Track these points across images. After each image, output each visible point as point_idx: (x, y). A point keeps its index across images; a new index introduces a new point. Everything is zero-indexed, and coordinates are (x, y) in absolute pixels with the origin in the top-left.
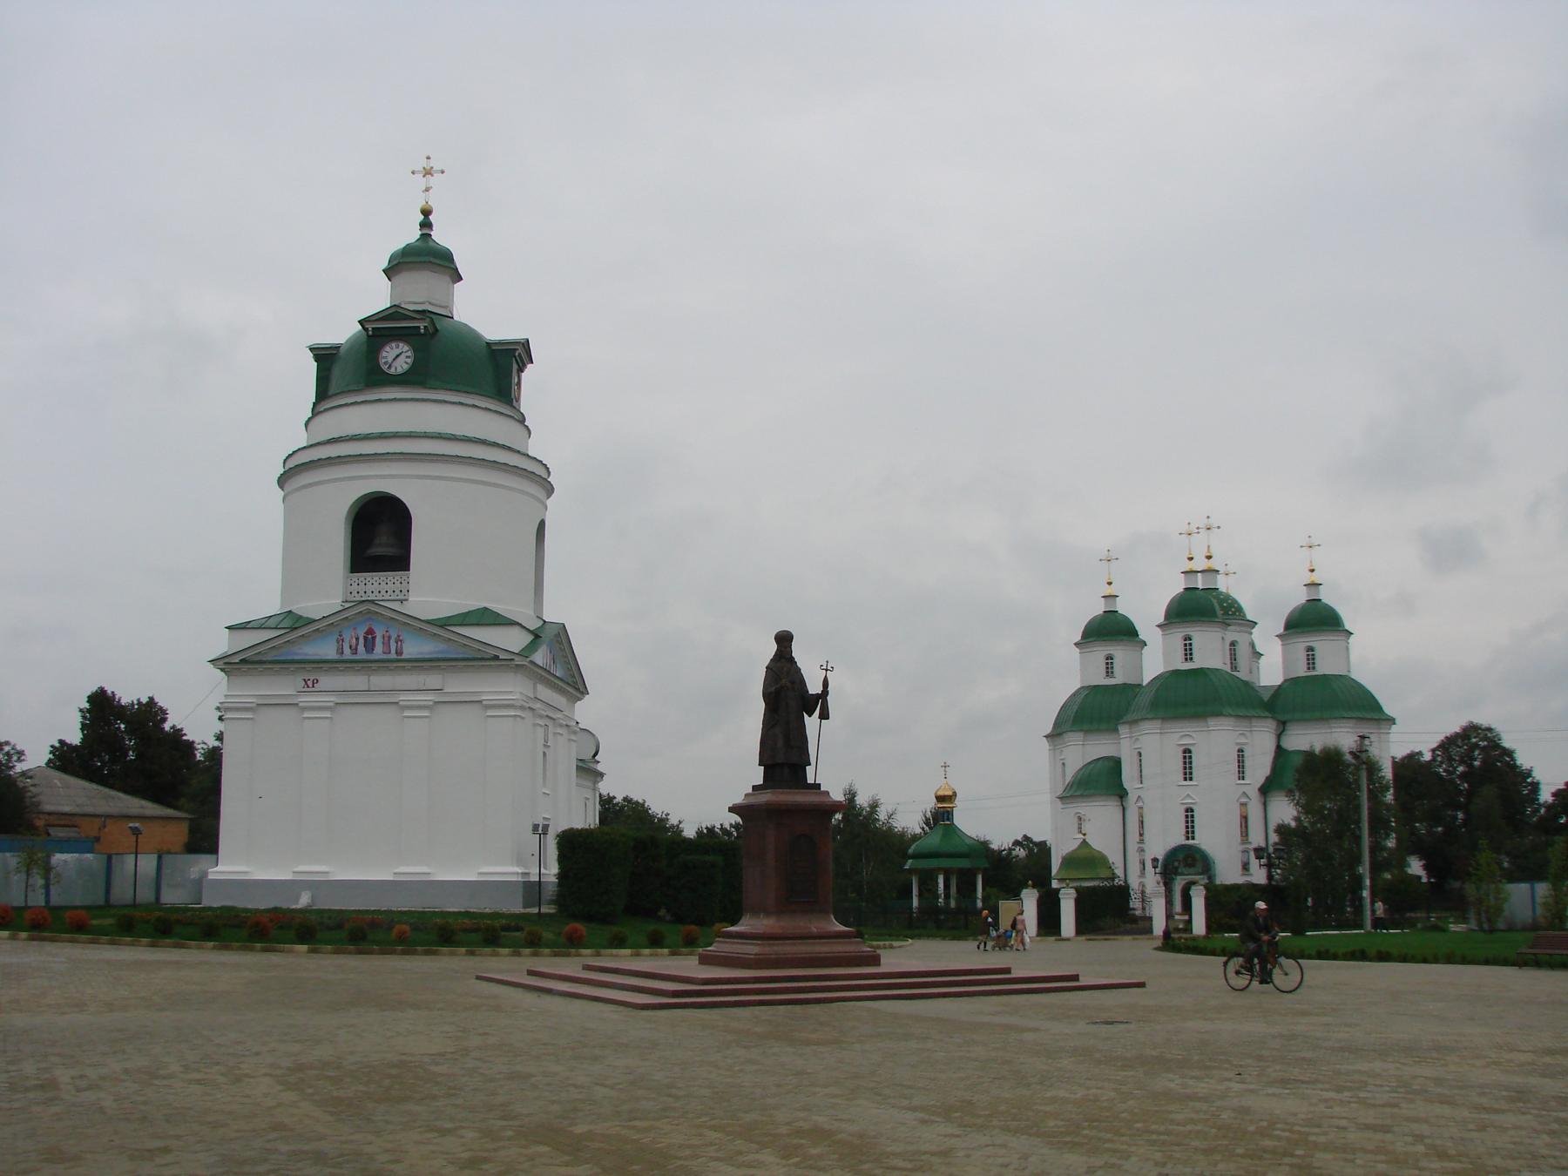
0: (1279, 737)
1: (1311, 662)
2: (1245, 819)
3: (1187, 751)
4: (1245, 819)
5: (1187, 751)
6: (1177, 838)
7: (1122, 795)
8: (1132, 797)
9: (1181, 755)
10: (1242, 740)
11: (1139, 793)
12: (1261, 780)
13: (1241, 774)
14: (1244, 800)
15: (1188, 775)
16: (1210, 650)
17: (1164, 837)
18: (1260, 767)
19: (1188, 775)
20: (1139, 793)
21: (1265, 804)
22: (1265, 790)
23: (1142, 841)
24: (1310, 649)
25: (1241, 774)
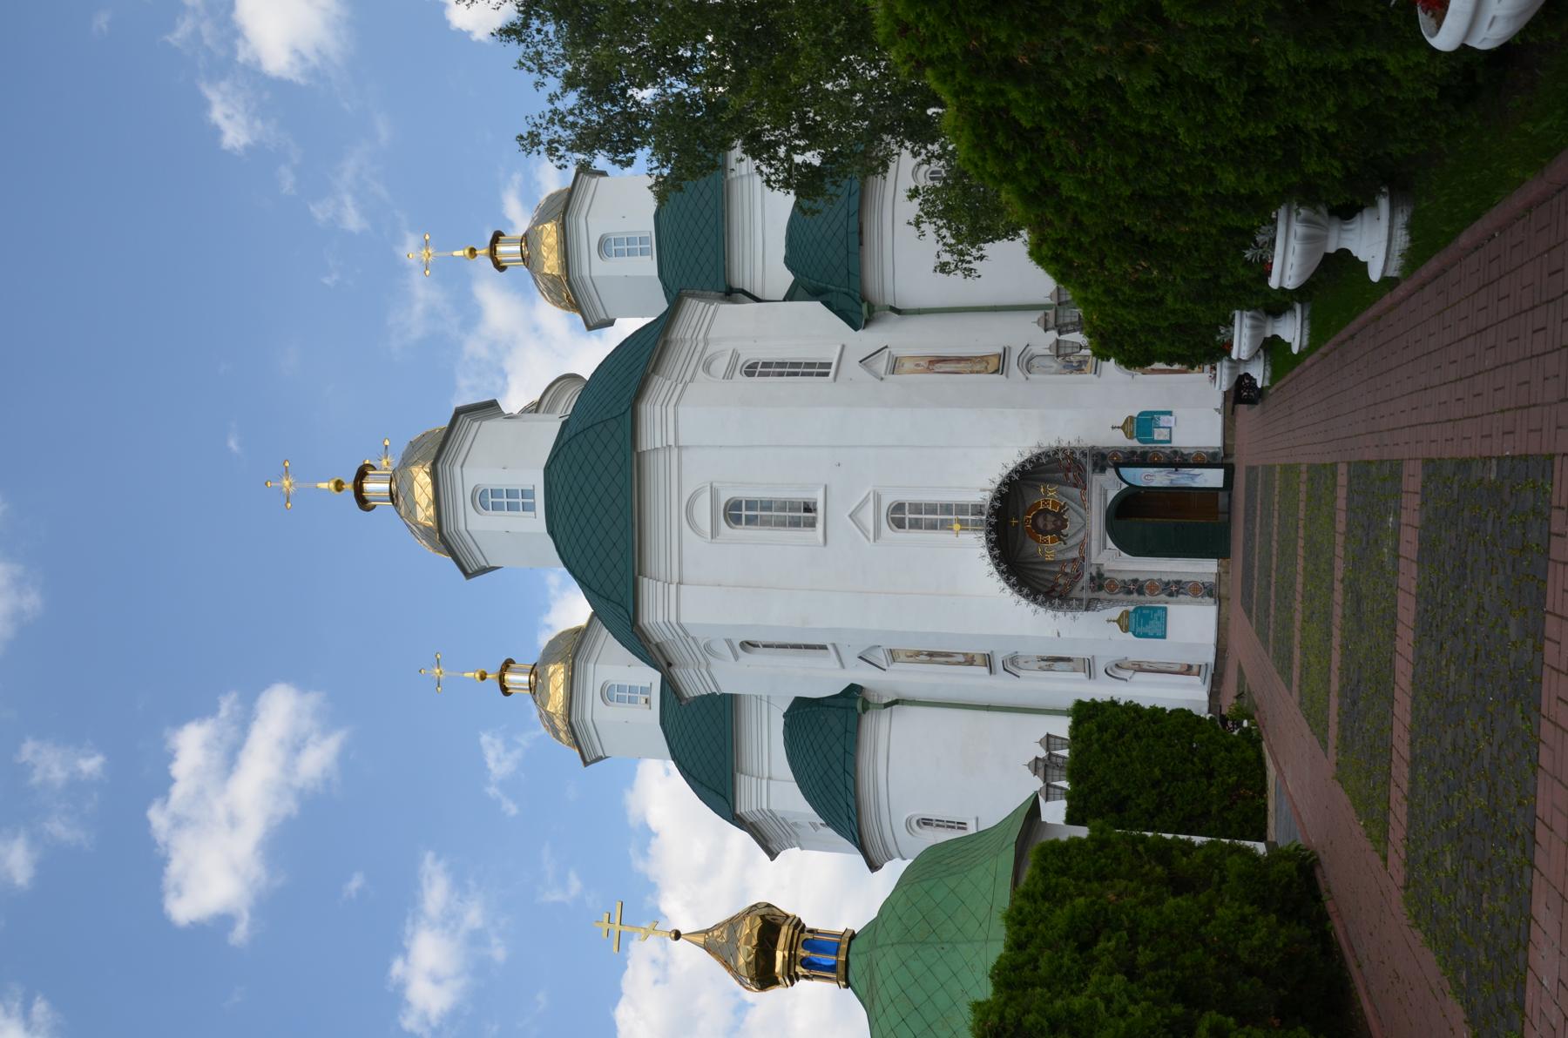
0: (758, 300)
2: (936, 363)
4: (936, 363)
5: (736, 513)
6: (970, 554)
8: (863, 675)
9: (742, 532)
10: (720, 366)
11: (850, 658)
13: (819, 369)
14: (882, 364)
18: (814, 328)
20: (850, 658)
23: (988, 661)
24: (603, 244)
25: (819, 369)
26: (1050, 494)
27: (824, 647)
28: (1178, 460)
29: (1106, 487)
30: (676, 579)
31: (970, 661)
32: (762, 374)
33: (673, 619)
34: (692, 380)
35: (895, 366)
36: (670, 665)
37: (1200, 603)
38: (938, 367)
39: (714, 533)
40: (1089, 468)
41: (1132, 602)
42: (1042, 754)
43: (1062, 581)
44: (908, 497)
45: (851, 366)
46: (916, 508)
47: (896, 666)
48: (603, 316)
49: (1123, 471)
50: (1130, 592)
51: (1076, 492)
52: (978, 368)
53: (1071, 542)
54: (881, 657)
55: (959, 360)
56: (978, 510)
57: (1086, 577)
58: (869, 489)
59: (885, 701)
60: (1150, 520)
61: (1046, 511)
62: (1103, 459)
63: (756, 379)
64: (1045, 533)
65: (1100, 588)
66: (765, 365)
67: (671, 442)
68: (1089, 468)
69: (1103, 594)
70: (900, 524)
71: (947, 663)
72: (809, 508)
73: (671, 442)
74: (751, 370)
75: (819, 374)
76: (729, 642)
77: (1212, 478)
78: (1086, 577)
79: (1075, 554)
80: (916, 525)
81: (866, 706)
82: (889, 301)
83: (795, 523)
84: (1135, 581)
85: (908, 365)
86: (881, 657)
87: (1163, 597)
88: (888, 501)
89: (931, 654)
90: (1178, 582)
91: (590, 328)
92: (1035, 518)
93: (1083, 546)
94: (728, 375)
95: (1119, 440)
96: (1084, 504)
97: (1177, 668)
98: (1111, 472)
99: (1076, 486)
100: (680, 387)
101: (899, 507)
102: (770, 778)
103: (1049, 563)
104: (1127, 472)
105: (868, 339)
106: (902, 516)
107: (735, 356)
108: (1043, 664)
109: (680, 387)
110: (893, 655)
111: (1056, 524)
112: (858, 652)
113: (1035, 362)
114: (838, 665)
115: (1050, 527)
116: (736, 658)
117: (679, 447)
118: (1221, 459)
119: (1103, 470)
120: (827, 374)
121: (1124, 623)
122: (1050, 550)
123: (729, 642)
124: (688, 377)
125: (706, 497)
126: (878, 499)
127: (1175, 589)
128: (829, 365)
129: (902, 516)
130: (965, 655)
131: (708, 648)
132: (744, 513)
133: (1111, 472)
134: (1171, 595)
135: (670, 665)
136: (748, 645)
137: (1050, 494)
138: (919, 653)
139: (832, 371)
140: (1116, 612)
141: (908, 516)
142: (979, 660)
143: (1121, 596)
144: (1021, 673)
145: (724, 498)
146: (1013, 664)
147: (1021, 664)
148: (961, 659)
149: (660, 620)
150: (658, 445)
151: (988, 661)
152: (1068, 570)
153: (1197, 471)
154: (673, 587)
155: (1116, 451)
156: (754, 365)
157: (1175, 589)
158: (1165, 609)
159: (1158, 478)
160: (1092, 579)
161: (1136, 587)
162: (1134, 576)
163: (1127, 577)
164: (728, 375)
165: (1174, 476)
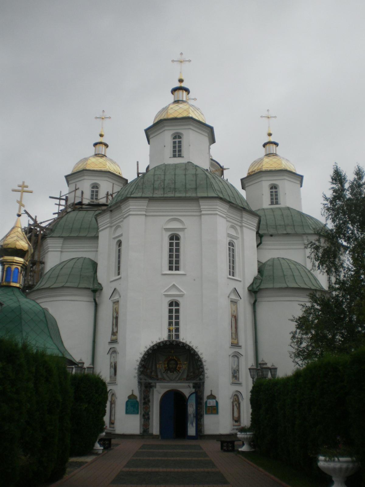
1: (275, 199)
2: (235, 318)
3: (175, 239)
4: (235, 318)
5: (175, 239)
6: (159, 334)
7: (96, 290)
8: (107, 291)
12: (249, 280)
13: (232, 271)
14: (233, 297)
15: (174, 263)
16: (196, 153)
17: (144, 333)
19: (174, 263)
21: (254, 305)
22: (255, 291)
23: (114, 341)
26: (184, 366)
27: (119, 274)
28: (199, 417)
29: (186, 389)
30: (147, 214)
31: (114, 333)
32: (229, 248)
33: (131, 213)
34: (227, 221)
35: (234, 302)
36: (111, 211)
37: (140, 428)
38: (233, 319)
39: (167, 230)
40: (194, 381)
41: (140, 400)
42: (269, 365)
43: (148, 371)
44: (182, 308)
45: (234, 285)
46: (177, 311)
47: (111, 304)
48: (246, 185)
49: (194, 396)
50: (144, 399)
51: (185, 376)
52: (234, 336)
53: (165, 375)
54: (116, 297)
55: (236, 328)
56: (177, 336)
57: (150, 381)
58: (185, 292)
59: (97, 299)
60: (175, 405)
61: (177, 364)
62: (199, 387)
63: (228, 246)
64: (168, 364)
65: (146, 387)
66: (233, 250)
67: (203, 212)
68: (194, 381)
69: (143, 388)
70: (171, 304)
71: (113, 325)
72: (177, 269)
73: (203, 212)
74: (231, 244)
75: (230, 271)
76: (121, 235)
77: (192, 431)
78: (150, 381)
79: (160, 376)
80: (170, 311)
81: (95, 291)
82: (259, 299)
83: (171, 262)
84: (149, 401)
85: (234, 307)
86: (116, 297)
87: (143, 413)
88: (179, 299)
89: (117, 318)
90: (149, 418)
91: (242, 180)
92: (173, 360)
93: (163, 380)
94: (229, 235)
95: (207, 393)
96: (180, 380)
97: (113, 418)
98: (193, 390)
99: (188, 376)
100: (224, 216)
101: (177, 304)
102: (61, 252)
103: (156, 366)
104: (194, 397)
105: (243, 292)
106: (174, 305)
107: (237, 238)
108: (113, 364)
109: (224, 216)
110: (116, 302)
111: (172, 368)
112: (118, 288)
113: (236, 359)
114: (112, 280)
115: (171, 366)
116: (114, 238)
117: (200, 215)
118: (200, 435)
119: (194, 387)
120: (230, 275)
121: (132, 397)
122: (161, 366)
123: (121, 235)
124: (228, 219)
125: (181, 227)
126: (181, 296)
127: (146, 418)
128: (233, 276)
129: (174, 305)
130: (117, 332)
131: (118, 227)
132: (174, 242)
133: (193, 390)
134: (144, 416)
135: (111, 211)
136: (120, 243)
137: (184, 366)
138: (117, 313)
139: (231, 277)
140: (137, 393)
141: (174, 308)
142: (114, 337)
143: (143, 396)
144: (109, 355)
145: (181, 234)
146: (113, 352)
147: (113, 355)
148: (115, 330)
149: (131, 207)
150: (202, 207)
151: (114, 341)
152: (153, 374)
153: (194, 425)
154: (144, 213)
155: (202, 392)
156: (233, 246)
157: (146, 418)
158: (138, 413)
159: (191, 409)
160: (150, 383)
161: (147, 401)
162: (151, 400)
163: (151, 398)
164: (229, 235)
165: (192, 416)
